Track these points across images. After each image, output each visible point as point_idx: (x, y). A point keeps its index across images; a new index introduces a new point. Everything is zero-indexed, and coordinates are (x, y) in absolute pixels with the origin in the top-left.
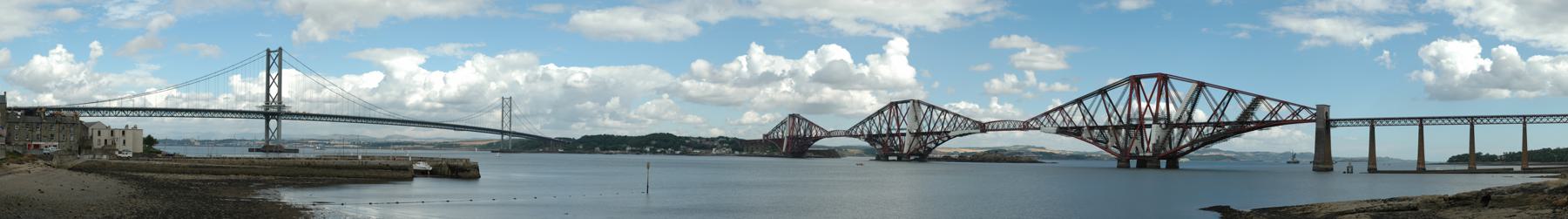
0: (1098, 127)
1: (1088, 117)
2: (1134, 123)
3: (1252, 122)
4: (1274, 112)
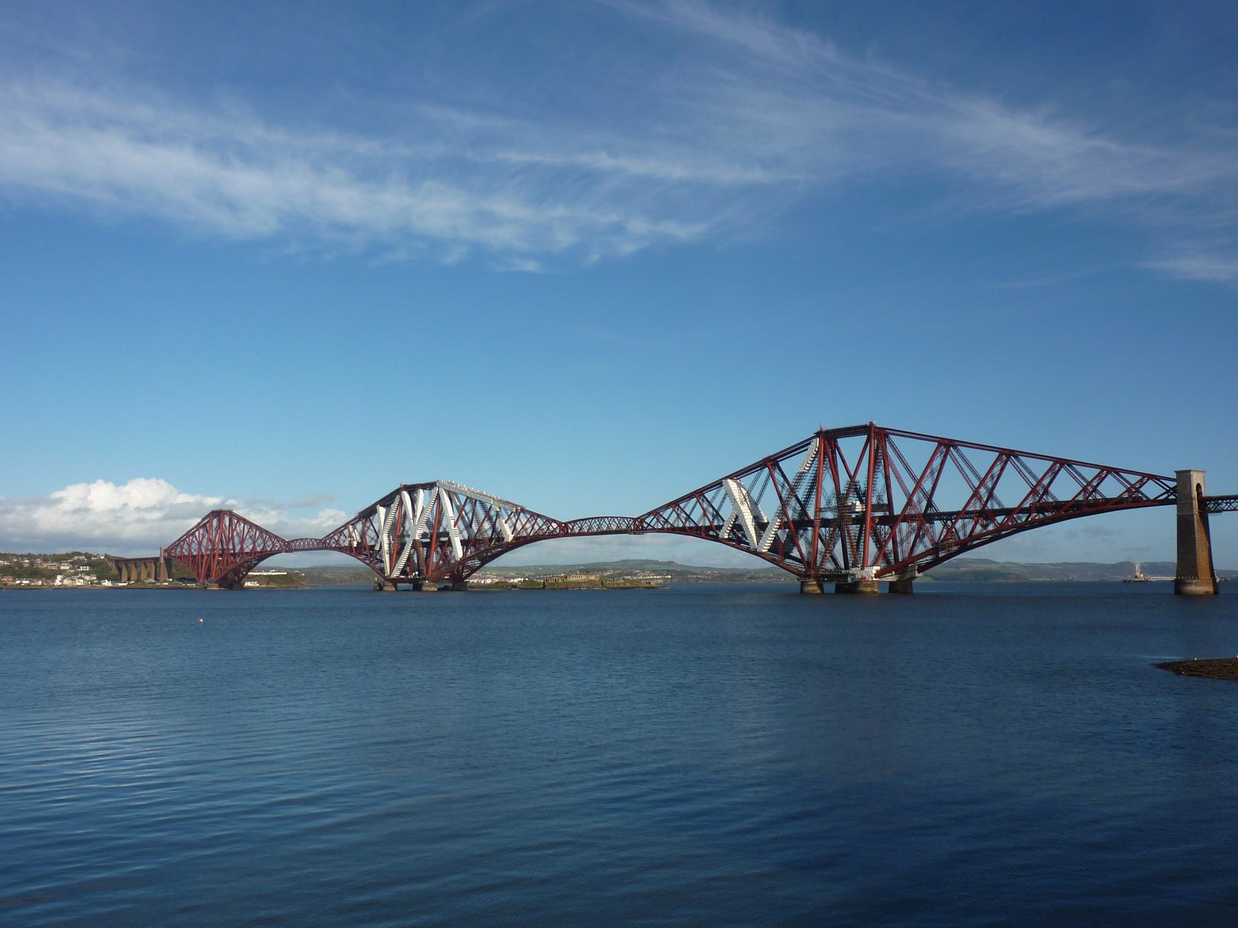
2: (830, 515)
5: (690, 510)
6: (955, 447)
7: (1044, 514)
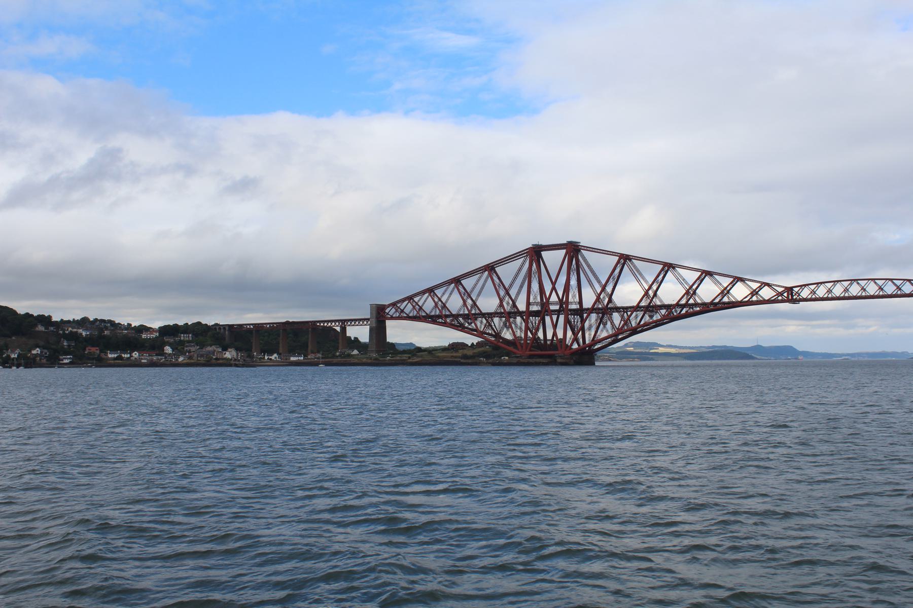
0: (483, 315)
1: (469, 302)
3: (696, 305)
4: (725, 292)
5: (428, 300)
6: (630, 260)
7: (693, 308)
